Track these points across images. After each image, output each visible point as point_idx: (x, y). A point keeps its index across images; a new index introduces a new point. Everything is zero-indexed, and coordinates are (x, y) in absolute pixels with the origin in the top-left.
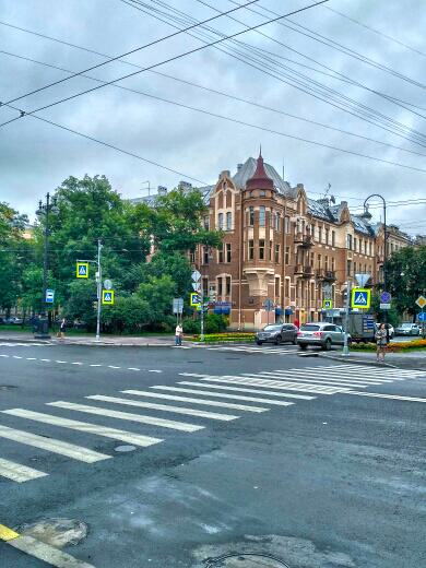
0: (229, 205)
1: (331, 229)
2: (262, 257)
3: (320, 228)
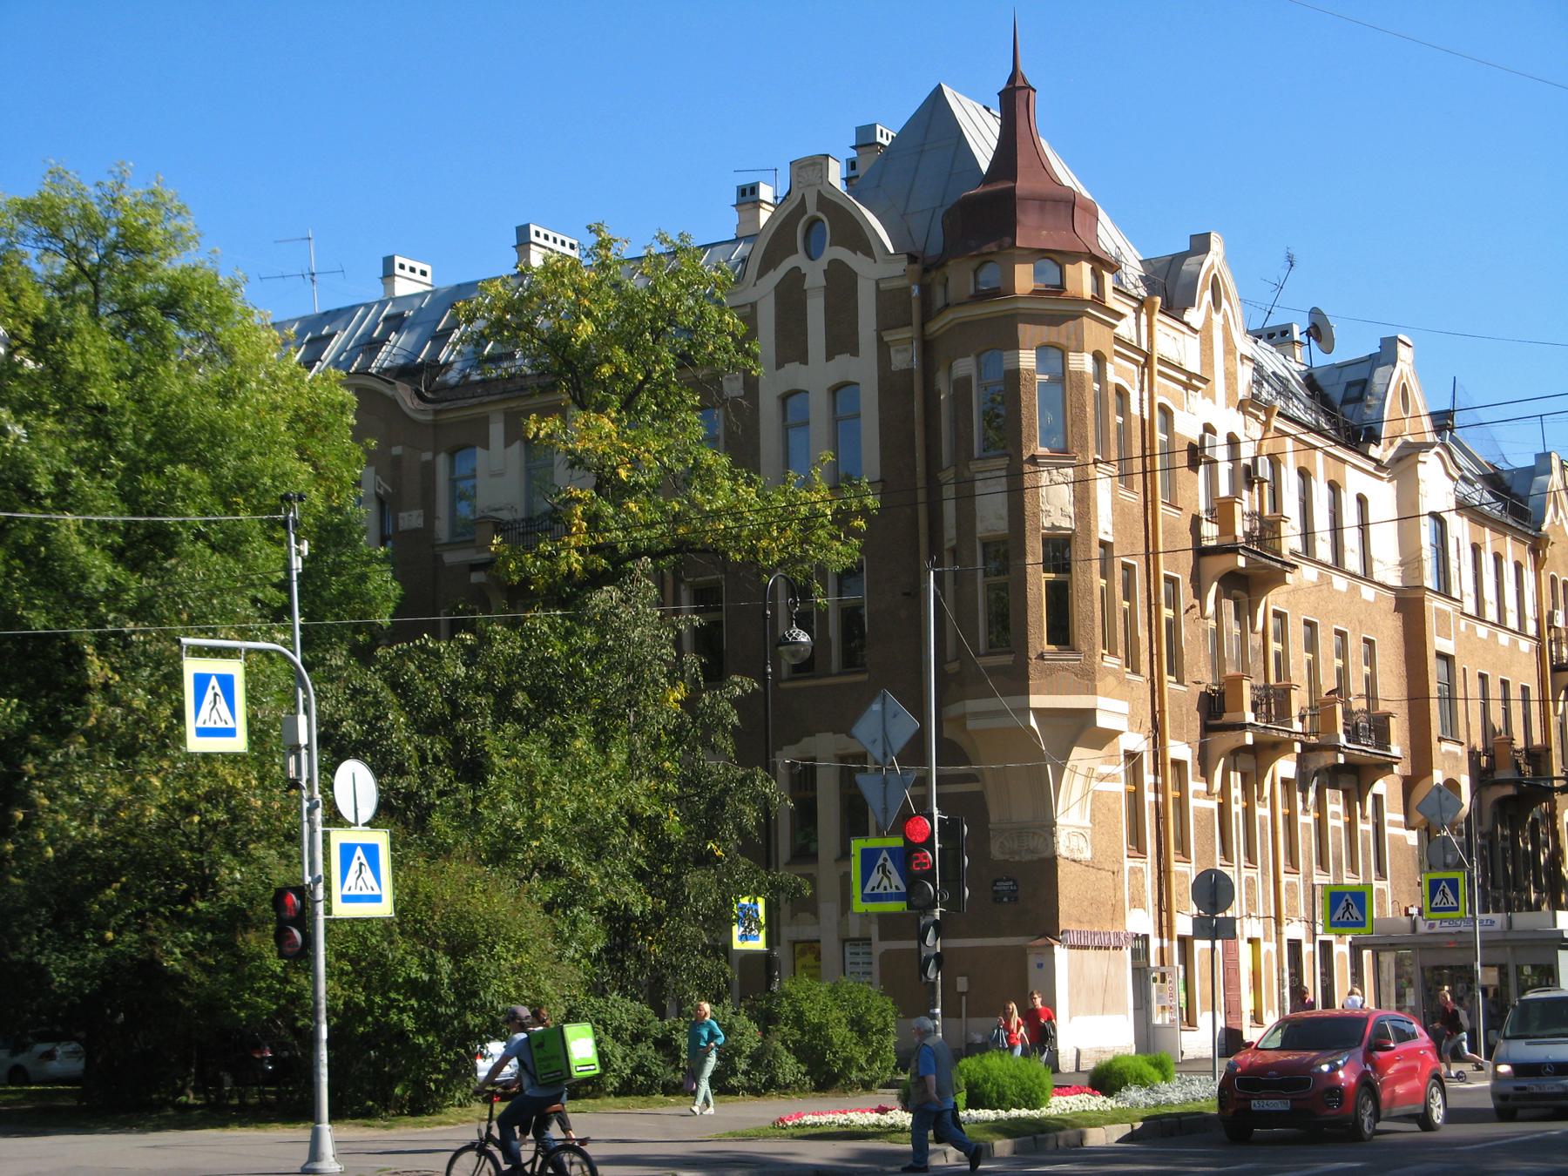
0: (842, 341)
2: (1061, 632)
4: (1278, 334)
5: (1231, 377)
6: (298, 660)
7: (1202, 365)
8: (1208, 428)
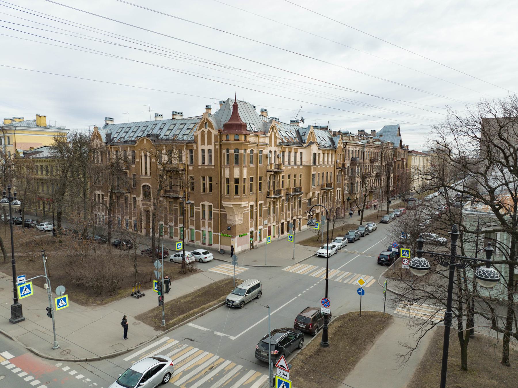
0: (209, 143)
1: (300, 151)
2: (237, 192)
5: (275, 142)
6: (46, 277)
8: (270, 152)
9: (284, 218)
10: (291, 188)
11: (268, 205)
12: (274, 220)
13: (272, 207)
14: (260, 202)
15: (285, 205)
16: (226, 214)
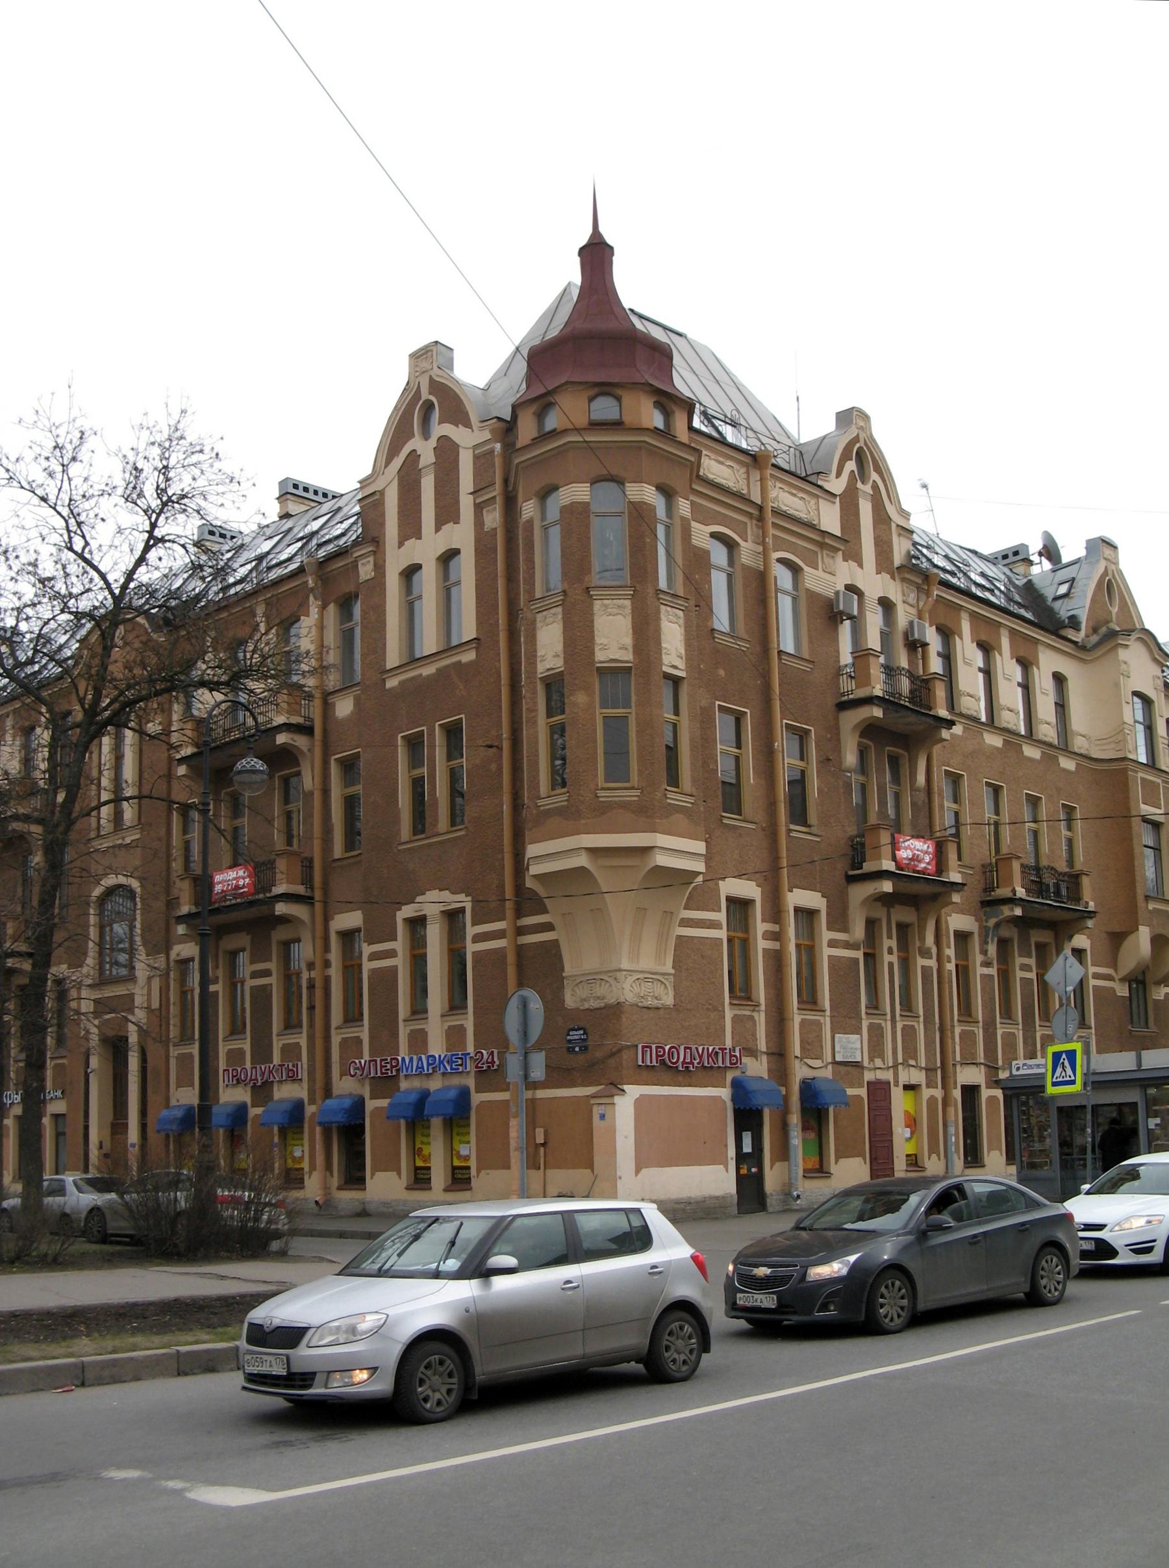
1: (1048, 662)
2: (617, 770)
3: (986, 648)
4: (1010, 555)
7: (843, 528)
9: (981, 1058)
10: (1009, 859)
11: (859, 931)
12: (910, 1051)
13: (889, 958)
14: (798, 898)
15: (981, 971)
16: (555, 944)
